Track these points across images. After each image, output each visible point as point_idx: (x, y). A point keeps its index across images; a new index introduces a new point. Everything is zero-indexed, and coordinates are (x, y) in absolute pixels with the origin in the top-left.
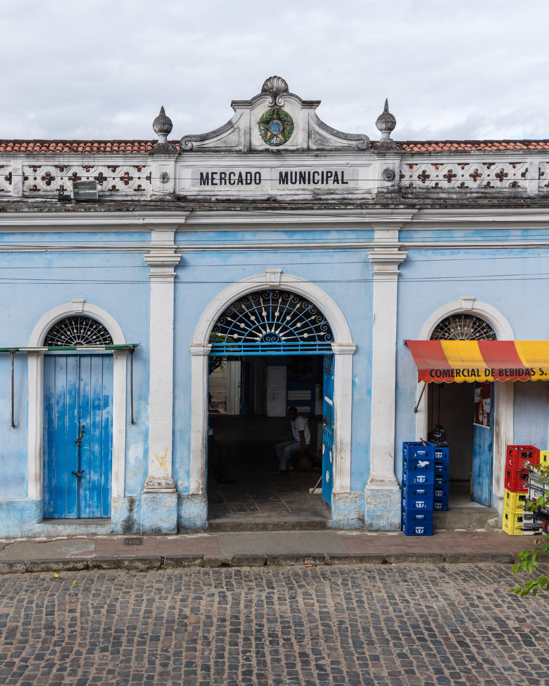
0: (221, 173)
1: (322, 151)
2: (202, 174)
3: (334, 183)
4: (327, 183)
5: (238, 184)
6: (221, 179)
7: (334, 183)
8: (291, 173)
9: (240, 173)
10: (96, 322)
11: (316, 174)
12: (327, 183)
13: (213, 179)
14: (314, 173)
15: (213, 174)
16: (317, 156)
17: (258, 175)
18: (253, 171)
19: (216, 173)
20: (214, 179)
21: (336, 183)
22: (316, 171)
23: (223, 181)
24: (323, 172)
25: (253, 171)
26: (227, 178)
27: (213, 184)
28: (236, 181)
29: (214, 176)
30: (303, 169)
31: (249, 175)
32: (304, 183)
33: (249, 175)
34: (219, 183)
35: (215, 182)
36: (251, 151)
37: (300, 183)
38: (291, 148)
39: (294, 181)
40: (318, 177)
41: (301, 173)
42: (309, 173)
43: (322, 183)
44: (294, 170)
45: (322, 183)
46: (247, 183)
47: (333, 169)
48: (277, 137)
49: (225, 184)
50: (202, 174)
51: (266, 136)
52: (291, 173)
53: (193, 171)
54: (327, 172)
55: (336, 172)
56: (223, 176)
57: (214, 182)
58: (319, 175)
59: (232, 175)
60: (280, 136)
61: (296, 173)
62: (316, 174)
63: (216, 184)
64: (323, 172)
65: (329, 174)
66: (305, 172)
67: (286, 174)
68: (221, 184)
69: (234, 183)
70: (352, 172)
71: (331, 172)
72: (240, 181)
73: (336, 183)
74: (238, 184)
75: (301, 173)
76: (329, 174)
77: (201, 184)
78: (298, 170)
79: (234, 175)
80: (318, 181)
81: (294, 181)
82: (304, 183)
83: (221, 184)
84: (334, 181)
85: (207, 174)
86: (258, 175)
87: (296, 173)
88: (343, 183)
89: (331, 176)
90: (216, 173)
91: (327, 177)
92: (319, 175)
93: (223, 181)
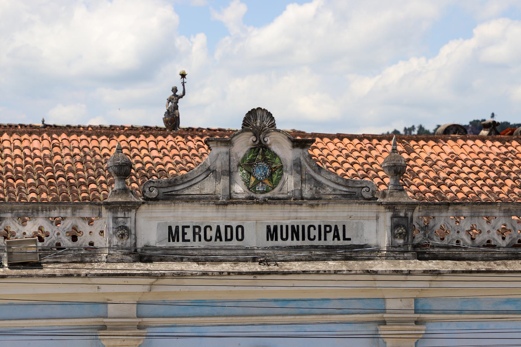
0: (194, 227)
2: (170, 228)
3: (333, 240)
4: (325, 239)
5: (216, 240)
6: (194, 233)
7: (333, 240)
8: (282, 226)
9: (218, 227)
11: (312, 228)
12: (325, 239)
13: (184, 234)
14: (310, 226)
15: (184, 227)
16: (312, 206)
17: (240, 229)
18: (234, 225)
19: (188, 227)
20: (186, 234)
21: (336, 239)
22: (312, 224)
23: (197, 237)
24: (320, 226)
25: (234, 225)
26: (202, 233)
27: (184, 240)
28: (214, 238)
29: (186, 230)
30: (295, 223)
31: (229, 229)
32: (298, 239)
33: (229, 229)
34: (192, 240)
35: (186, 237)
36: (230, 200)
37: (292, 239)
38: (281, 196)
39: (284, 237)
40: (314, 233)
41: (293, 227)
42: (303, 227)
43: (320, 239)
44: (285, 223)
45: (320, 239)
46: (226, 240)
48: (263, 183)
49: (200, 240)
50: (170, 228)
51: (249, 182)
52: (282, 226)
53: (159, 224)
54: (326, 226)
55: (336, 226)
56: (197, 230)
57: (186, 238)
58: (315, 229)
59: (208, 229)
60: (266, 181)
61: (287, 226)
62: (312, 228)
63: (189, 241)
64: (320, 226)
65: (328, 229)
66: (298, 226)
67: (275, 227)
68: (194, 240)
69: (211, 240)
70: (355, 225)
71: (330, 226)
72: (219, 237)
73: (336, 239)
74: (216, 240)
75: (293, 227)
76: (328, 229)
77: (169, 241)
78: (289, 223)
79: (211, 230)
80: (315, 236)
81: (284, 237)
82: (298, 239)
83: (194, 240)
84: (334, 237)
85: (177, 227)
86: (240, 229)
87: (287, 226)
88: (345, 239)
89: (330, 231)
90: (188, 227)
91: (326, 232)
92: (315, 229)
93: (197, 237)
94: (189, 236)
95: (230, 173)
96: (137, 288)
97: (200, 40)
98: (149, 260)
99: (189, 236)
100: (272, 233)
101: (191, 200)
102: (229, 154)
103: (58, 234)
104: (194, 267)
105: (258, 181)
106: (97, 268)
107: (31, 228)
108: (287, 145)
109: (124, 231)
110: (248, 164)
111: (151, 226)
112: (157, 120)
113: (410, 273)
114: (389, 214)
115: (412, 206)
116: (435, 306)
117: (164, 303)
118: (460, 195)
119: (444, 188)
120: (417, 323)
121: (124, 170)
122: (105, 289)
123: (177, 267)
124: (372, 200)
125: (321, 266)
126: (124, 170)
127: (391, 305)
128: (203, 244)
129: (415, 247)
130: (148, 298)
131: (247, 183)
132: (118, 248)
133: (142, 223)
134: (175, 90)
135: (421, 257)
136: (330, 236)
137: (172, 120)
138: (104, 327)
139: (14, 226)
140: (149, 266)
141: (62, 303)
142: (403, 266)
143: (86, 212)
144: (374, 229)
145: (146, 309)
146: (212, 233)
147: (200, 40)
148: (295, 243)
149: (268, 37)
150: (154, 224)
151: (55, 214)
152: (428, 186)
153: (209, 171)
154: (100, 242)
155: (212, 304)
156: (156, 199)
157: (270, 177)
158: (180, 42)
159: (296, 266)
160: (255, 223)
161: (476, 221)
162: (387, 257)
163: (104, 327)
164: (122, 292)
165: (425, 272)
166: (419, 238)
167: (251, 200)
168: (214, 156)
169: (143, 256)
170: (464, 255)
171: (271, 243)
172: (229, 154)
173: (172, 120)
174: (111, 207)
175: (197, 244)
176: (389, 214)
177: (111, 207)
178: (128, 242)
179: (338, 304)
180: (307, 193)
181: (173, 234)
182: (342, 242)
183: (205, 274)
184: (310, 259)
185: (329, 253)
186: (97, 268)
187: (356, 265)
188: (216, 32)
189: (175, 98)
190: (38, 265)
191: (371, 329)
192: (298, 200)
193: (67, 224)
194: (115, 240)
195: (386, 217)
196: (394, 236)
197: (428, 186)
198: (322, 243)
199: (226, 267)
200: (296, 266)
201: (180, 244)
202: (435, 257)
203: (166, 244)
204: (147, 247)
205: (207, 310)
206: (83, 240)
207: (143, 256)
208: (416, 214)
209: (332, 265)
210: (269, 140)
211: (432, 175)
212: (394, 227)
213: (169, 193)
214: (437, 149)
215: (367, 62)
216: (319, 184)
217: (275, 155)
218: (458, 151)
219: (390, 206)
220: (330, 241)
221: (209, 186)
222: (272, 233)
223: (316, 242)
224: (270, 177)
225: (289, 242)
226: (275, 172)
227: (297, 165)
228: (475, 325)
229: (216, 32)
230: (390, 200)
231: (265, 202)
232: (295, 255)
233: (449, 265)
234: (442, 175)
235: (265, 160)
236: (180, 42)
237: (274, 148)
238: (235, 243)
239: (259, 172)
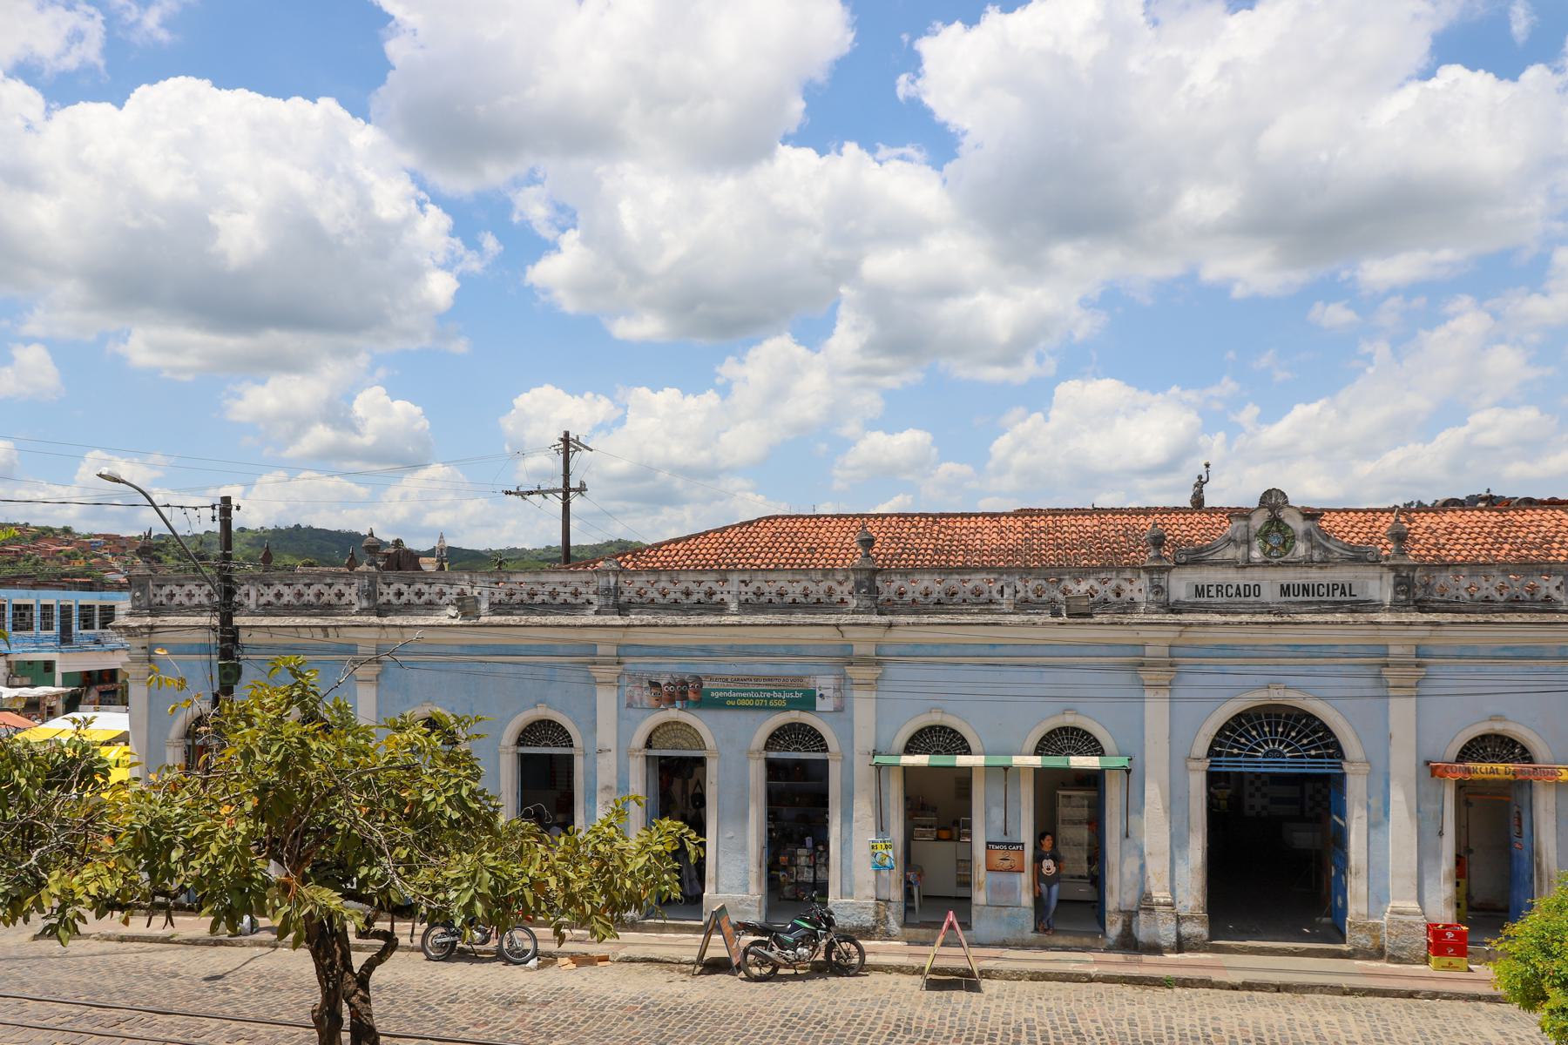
1: (1324, 563)
10: (1086, 733)
18: (1252, 583)
25: (1252, 583)
36: (1249, 564)
40: (1322, 590)
47: (1339, 581)
78: (1301, 582)
94: (1213, 592)
95: (1248, 542)
96: (1170, 634)
97: (1221, 436)
98: (1180, 612)
99: (1213, 592)
100: (1285, 590)
101: (1215, 564)
102: (1247, 527)
103: (1105, 591)
104: (1217, 618)
105: (1272, 548)
106: (1136, 618)
107: (1084, 587)
108: (1299, 518)
109: (1158, 589)
110: (1264, 535)
111: (1180, 585)
112: (1185, 501)
113: (1411, 624)
114: (1392, 574)
115: (1413, 568)
116: (1435, 652)
117: (1192, 646)
118: (1459, 558)
119: (1444, 552)
120: (1418, 665)
121: (1158, 541)
122: (1143, 634)
123: (1202, 617)
124: (1376, 562)
125: (1329, 618)
126: (1158, 541)
127: (1393, 650)
128: (1225, 599)
129: (1416, 602)
130: (1178, 642)
131: (1263, 550)
132: (1153, 602)
133: (1173, 582)
134: (1200, 477)
135: (1422, 610)
136: (1338, 593)
137: (1198, 501)
138: (1142, 665)
139: (1071, 585)
140: (1179, 617)
141: (1108, 645)
142: (1404, 618)
143: (1128, 575)
144: (1379, 587)
145: (1176, 651)
146: (1232, 591)
147: (1221, 436)
148: (1306, 598)
149: (1277, 432)
150: (1184, 584)
151: (1103, 576)
152: (1429, 550)
153: (1230, 540)
154: (1139, 597)
155: (1233, 647)
156: (1185, 564)
157: (1284, 545)
158: (1203, 440)
159: (1307, 618)
160: (1270, 583)
161: (1475, 580)
162: (1390, 611)
163: (1142, 665)
164: (1157, 637)
165: (1426, 623)
166: (1420, 594)
167: (1266, 564)
168: (1232, 528)
169: (1174, 608)
170: (1463, 607)
171: (1284, 599)
172: (1247, 527)
173: (1198, 501)
174: (1148, 570)
175: (1219, 600)
176: (1392, 574)
177: (1148, 570)
178: (1162, 598)
179: (1344, 650)
180: (1316, 556)
181: (1199, 591)
182: (1348, 598)
183: (1226, 623)
184: (1319, 612)
185: (1337, 607)
186: (1136, 618)
187: (1361, 617)
188: (1233, 430)
189: (1200, 484)
190: (1090, 615)
191: (1376, 669)
192: (1309, 563)
193: (1113, 583)
194: (1151, 597)
195: (1390, 577)
196: (1396, 593)
197: (1429, 550)
198: (1330, 598)
199: (1245, 618)
200: (1307, 618)
201: (1206, 599)
202: (1435, 611)
203: (1193, 600)
204: (1177, 602)
205: (1228, 653)
206: (1126, 596)
207: (1174, 608)
208: (1417, 574)
209: (1339, 617)
210: (1282, 515)
211: (1432, 541)
212: (1397, 585)
213: (1196, 558)
214: (1437, 519)
215: (1367, 449)
216: (1327, 550)
217: (1288, 527)
218: (1456, 520)
219: (1393, 568)
220: (1338, 597)
221: (1230, 553)
222: (1285, 590)
223: (1325, 598)
224: (1284, 545)
225: (1300, 598)
226: (1288, 540)
227: (1308, 535)
228: (1473, 669)
229: (1233, 430)
230: (1393, 562)
231: (1278, 565)
232: (1305, 609)
233: (1449, 617)
234: (1442, 541)
235: (1279, 531)
236: (1203, 440)
237: (1287, 521)
238: (1252, 599)
239: (1274, 540)
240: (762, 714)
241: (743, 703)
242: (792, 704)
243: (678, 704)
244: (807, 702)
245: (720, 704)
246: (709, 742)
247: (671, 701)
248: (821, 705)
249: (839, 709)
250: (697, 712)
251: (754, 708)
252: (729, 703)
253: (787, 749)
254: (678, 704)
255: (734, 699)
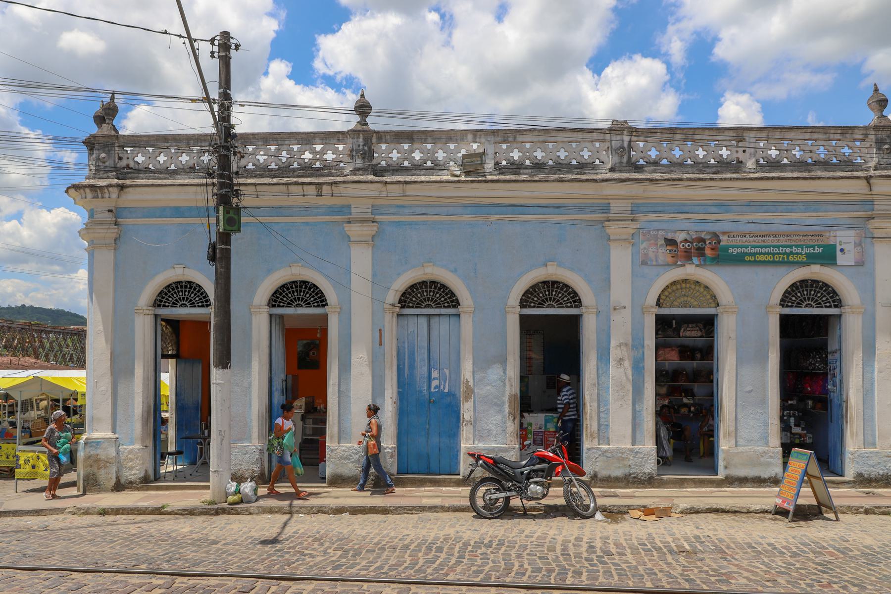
240: (782, 270)
241: (762, 258)
242: (812, 259)
243: (695, 260)
244: (828, 257)
245: (739, 260)
246: (725, 294)
247: (688, 256)
248: (841, 259)
249: (860, 264)
250: (716, 268)
251: (774, 263)
252: (747, 258)
253: (799, 305)
254: (695, 260)
255: (754, 254)
